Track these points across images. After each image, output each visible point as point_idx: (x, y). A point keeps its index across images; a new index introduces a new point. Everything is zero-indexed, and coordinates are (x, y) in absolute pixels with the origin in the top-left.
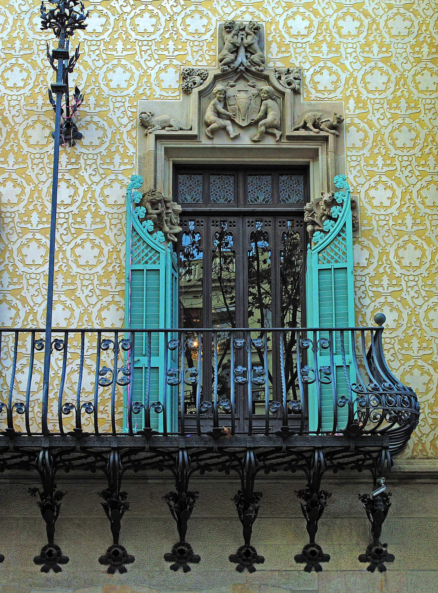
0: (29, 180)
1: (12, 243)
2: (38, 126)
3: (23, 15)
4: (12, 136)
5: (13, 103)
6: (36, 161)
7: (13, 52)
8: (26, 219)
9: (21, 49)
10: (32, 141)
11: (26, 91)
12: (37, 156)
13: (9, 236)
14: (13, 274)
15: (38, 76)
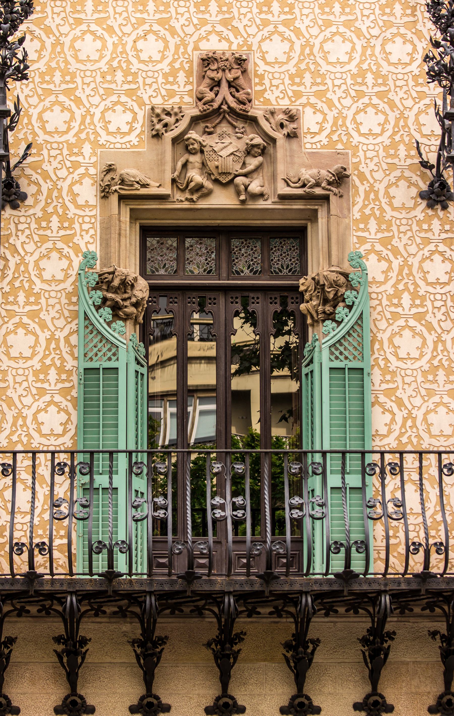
0: (396, 252)
1: (381, 332)
2: (403, 184)
3: (373, 41)
4: (372, 196)
5: (370, 154)
6: (402, 229)
7: (364, 88)
8: (395, 301)
9: (374, 85)
10: (397, 203)
11: (385, 139)
12: (404, 222)
13: (376, 322)
14: (385, 371)
15: (397, 120)
